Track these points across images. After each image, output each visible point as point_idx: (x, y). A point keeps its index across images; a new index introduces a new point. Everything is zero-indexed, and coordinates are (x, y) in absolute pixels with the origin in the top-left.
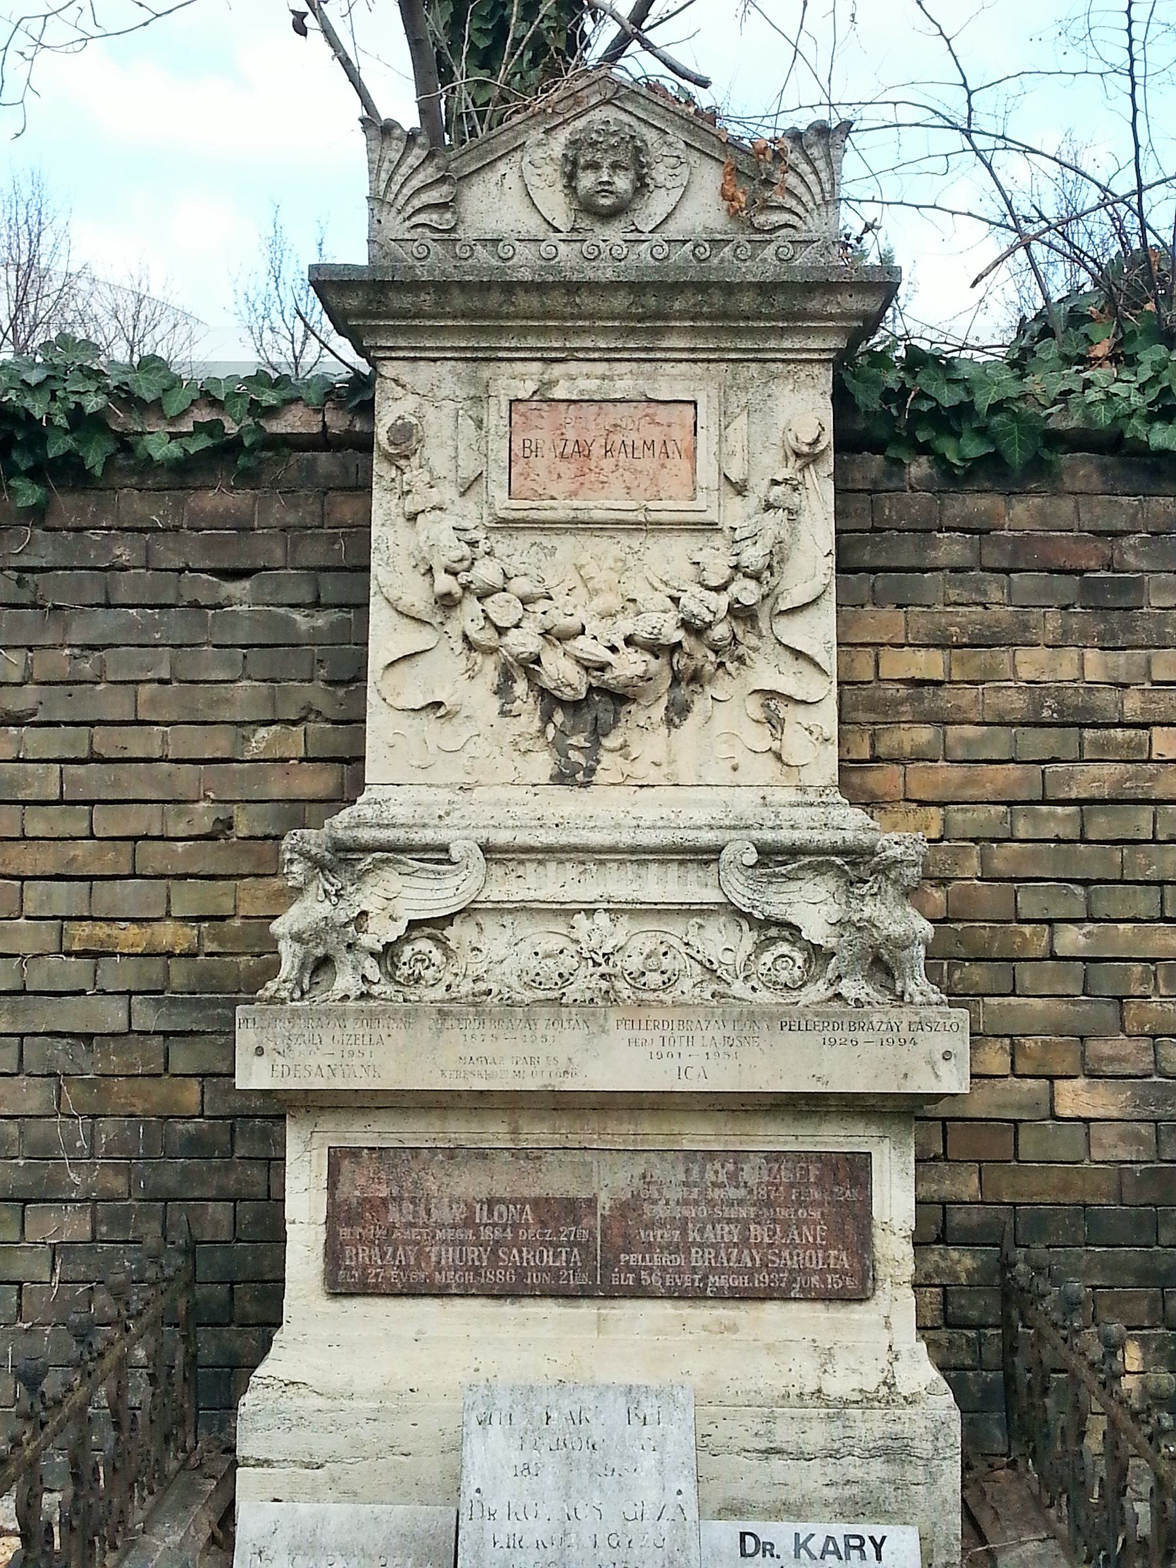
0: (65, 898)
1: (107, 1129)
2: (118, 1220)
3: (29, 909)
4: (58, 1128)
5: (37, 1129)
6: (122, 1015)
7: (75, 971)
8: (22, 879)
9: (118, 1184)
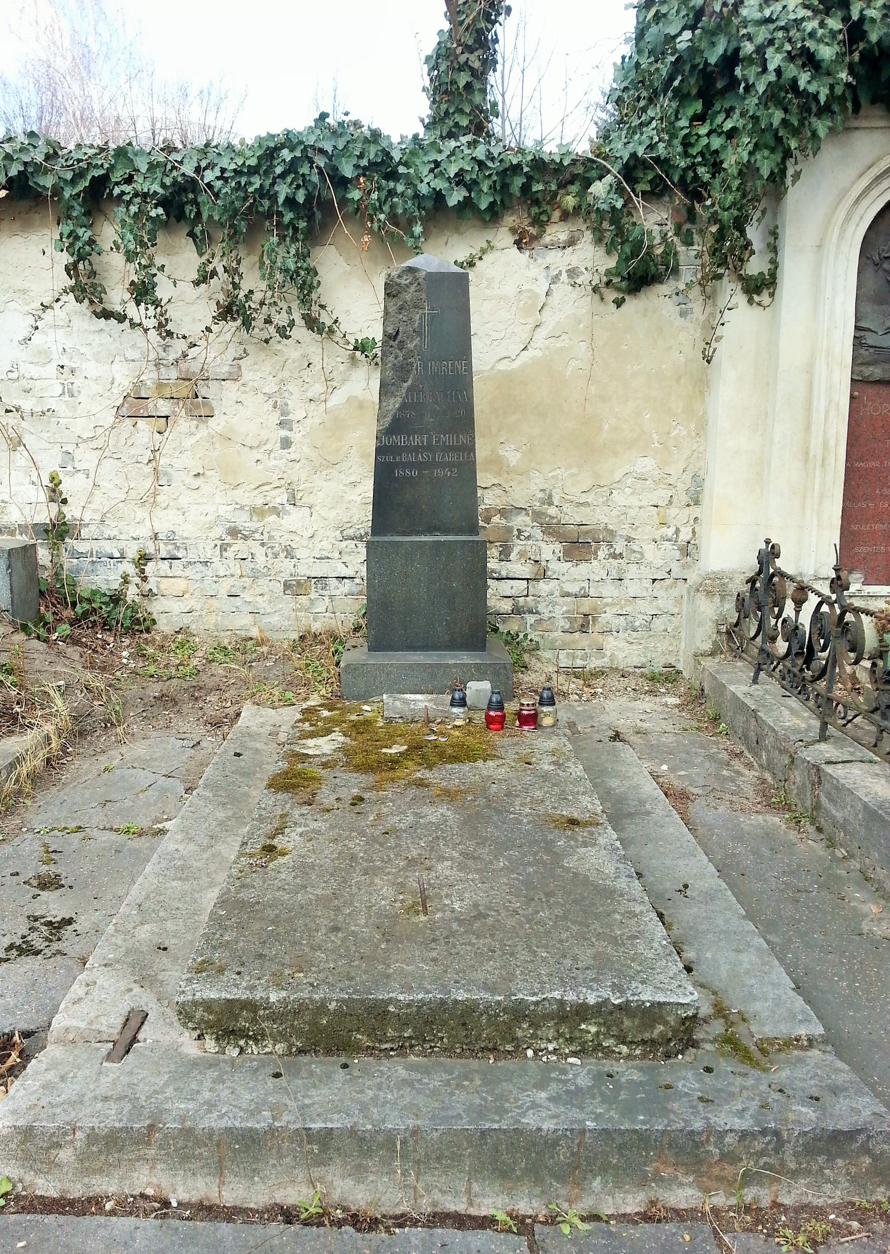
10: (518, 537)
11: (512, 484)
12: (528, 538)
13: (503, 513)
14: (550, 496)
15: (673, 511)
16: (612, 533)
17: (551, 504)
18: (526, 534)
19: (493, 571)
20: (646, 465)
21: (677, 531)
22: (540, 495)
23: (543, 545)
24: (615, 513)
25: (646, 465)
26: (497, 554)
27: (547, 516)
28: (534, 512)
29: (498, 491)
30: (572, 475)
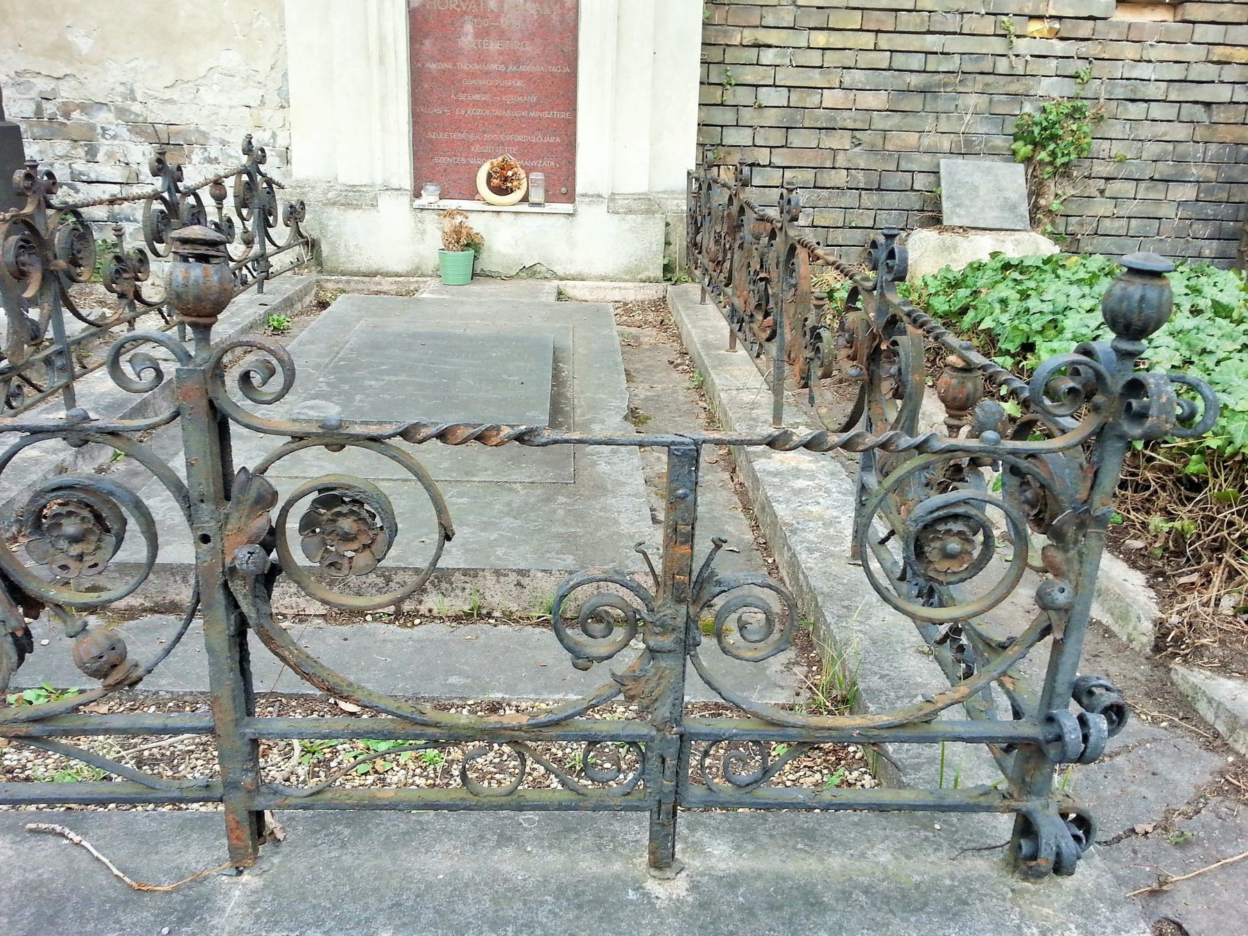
0: (1213, 34)
1: (1213, 148)
2: (1209, 191)
3: (1196, 39)
4: (1190, 147)
5: (1181, 147)
6: (1229, 94)
7: (1211, 72)
8: (1194, 23)
9: (1212, 174)
10: (103, 136)
11: (86, 74)
12: (114, 137)
13: (83, 108)
14: (132, 91)
15: (267, 113)
16: (204, 134)
17: (134, 100)
18: (112, 133)
19: (81, 173)
20: (232, 59)
21: (274, 136)
22: (121, 89)
23: (131, 145)
24: (205, 112)
25: (232, 59)
26: (83, 154)
27: (132, 113)
28: (116, 108)
29: (73, 82)
30: (152, 68)
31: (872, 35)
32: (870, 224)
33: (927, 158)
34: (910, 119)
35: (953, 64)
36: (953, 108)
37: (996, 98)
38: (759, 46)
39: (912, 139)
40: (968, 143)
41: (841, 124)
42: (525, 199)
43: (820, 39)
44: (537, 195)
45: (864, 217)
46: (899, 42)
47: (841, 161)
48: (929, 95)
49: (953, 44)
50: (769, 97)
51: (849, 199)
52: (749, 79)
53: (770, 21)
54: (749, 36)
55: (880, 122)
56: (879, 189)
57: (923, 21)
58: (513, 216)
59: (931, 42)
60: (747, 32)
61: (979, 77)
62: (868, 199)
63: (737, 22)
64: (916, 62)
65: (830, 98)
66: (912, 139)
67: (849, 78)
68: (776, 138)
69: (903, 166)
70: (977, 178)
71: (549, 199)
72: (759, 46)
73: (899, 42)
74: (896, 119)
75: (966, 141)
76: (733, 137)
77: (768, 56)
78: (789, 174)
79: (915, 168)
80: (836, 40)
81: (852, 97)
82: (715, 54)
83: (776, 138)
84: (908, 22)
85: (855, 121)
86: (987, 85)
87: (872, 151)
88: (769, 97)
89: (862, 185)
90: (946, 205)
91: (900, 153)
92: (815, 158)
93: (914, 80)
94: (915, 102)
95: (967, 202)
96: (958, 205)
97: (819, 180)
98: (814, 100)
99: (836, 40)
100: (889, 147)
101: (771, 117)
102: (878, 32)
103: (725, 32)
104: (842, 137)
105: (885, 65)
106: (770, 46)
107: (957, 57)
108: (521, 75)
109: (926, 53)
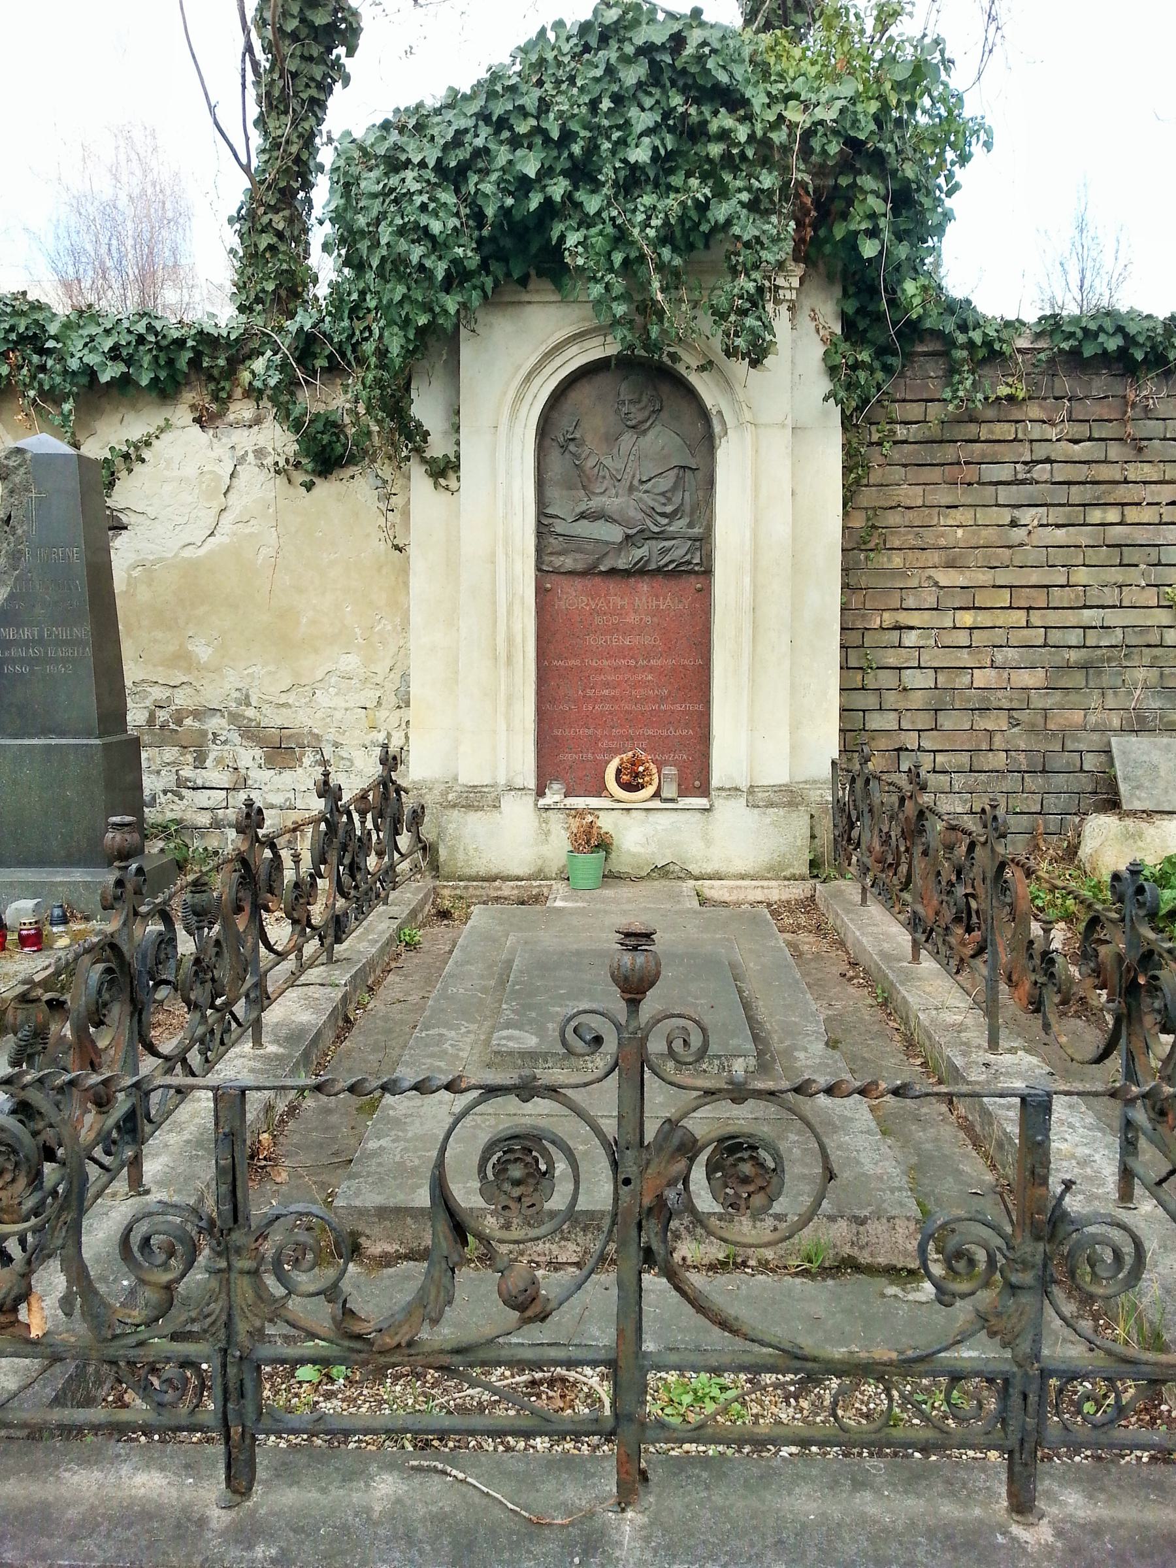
10: (214, 742)
11: (203, 682)
12: (225, 743)
13: (197, 714)
14: (247, 696)
15: (382, 714)
16: (317, 737)
17: (248, 705)
18: (223, 738)
19: (187, 780)
20: (351, 662)
21: (389, 736)
22: (237, 695)
23: (241, 750)
24: (319, 715)
25: (351, 662)
26: (191, 760)
27: (245, 718)
28: (230, 713)
29: (189, 690)
30: (270, 673)
31: (1023, 613)
32: (1037, 808)
33: (1095, 737)
34: (1073, 697)
35: (1116, 637)
36: (1120, 683)
37: (1167, 671)
38: (901, 628)
39: (1077, 717)
40: (1141, 719)
41: (995, 704)
42: (657, 794)
43: (967, 618)
44: (670, 791)
45: (1029, 802)
46: (1053, 618)
47: (998, 742)
48: (1091, 671)
49: (1113, 618)
50: (913, 679)
51: (1011, 782)
52: (892, 662)
53: (910, 602)
54: (888, 619)
55: (1038, 701)
56: (1043, 771)
57: (1077, 597)
58: (644, 813)
59: (1088, 616)
60: (886, 615)
61: (1146, 650)
62: (1030, 782)
63: (877, 605)
64: (1074, 638)
65: (981, 678)
66: (1077, 717)
67: (1000, 657)
68: (924, 721)
69: (1070, 745)
70: (1156, 757)
71: (683, 793)
72: (901, 628)
73: (1053, 618)
74: (1057, 696)
75: (1138, 717)
76: (876, 722)
77: (911, 638)
78: (940, 758)
79: (1082, 747)
80: (984, 619)
81: (1006, 675)
82: (854, 638)
83: (924, 721)
84: (1061, 599)
85: (1011, 700)
86: (1156, 657)
87: (1032, 730)
88: (913, 679)
89: (1024, 768)
90: (1123, 788)
91: (1064, 734)
92: (970, 740)
93: (1074, 656)
94: (1078, 679)
95: (1147, 784)
96: (1137, 788)
97: (975, 763)
98: (966, 680)
99: (984, 619)
100: (1053, 727)
101: (917, 700)
102: (1029, 609)
103: (863, 616)
104: (998, 717)
105: (1040, 642)
106: (912, 628)
107: (1119, 631)
108: (651, 669)
109: (1084, 628)
